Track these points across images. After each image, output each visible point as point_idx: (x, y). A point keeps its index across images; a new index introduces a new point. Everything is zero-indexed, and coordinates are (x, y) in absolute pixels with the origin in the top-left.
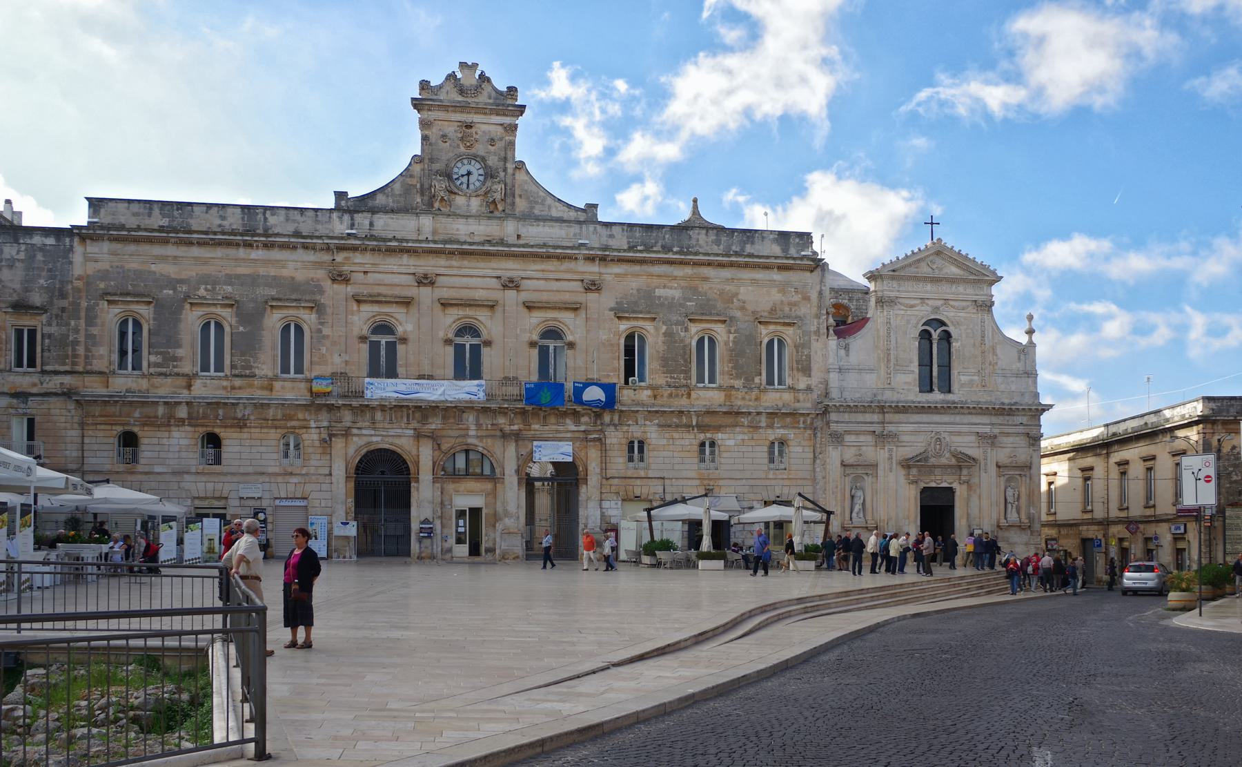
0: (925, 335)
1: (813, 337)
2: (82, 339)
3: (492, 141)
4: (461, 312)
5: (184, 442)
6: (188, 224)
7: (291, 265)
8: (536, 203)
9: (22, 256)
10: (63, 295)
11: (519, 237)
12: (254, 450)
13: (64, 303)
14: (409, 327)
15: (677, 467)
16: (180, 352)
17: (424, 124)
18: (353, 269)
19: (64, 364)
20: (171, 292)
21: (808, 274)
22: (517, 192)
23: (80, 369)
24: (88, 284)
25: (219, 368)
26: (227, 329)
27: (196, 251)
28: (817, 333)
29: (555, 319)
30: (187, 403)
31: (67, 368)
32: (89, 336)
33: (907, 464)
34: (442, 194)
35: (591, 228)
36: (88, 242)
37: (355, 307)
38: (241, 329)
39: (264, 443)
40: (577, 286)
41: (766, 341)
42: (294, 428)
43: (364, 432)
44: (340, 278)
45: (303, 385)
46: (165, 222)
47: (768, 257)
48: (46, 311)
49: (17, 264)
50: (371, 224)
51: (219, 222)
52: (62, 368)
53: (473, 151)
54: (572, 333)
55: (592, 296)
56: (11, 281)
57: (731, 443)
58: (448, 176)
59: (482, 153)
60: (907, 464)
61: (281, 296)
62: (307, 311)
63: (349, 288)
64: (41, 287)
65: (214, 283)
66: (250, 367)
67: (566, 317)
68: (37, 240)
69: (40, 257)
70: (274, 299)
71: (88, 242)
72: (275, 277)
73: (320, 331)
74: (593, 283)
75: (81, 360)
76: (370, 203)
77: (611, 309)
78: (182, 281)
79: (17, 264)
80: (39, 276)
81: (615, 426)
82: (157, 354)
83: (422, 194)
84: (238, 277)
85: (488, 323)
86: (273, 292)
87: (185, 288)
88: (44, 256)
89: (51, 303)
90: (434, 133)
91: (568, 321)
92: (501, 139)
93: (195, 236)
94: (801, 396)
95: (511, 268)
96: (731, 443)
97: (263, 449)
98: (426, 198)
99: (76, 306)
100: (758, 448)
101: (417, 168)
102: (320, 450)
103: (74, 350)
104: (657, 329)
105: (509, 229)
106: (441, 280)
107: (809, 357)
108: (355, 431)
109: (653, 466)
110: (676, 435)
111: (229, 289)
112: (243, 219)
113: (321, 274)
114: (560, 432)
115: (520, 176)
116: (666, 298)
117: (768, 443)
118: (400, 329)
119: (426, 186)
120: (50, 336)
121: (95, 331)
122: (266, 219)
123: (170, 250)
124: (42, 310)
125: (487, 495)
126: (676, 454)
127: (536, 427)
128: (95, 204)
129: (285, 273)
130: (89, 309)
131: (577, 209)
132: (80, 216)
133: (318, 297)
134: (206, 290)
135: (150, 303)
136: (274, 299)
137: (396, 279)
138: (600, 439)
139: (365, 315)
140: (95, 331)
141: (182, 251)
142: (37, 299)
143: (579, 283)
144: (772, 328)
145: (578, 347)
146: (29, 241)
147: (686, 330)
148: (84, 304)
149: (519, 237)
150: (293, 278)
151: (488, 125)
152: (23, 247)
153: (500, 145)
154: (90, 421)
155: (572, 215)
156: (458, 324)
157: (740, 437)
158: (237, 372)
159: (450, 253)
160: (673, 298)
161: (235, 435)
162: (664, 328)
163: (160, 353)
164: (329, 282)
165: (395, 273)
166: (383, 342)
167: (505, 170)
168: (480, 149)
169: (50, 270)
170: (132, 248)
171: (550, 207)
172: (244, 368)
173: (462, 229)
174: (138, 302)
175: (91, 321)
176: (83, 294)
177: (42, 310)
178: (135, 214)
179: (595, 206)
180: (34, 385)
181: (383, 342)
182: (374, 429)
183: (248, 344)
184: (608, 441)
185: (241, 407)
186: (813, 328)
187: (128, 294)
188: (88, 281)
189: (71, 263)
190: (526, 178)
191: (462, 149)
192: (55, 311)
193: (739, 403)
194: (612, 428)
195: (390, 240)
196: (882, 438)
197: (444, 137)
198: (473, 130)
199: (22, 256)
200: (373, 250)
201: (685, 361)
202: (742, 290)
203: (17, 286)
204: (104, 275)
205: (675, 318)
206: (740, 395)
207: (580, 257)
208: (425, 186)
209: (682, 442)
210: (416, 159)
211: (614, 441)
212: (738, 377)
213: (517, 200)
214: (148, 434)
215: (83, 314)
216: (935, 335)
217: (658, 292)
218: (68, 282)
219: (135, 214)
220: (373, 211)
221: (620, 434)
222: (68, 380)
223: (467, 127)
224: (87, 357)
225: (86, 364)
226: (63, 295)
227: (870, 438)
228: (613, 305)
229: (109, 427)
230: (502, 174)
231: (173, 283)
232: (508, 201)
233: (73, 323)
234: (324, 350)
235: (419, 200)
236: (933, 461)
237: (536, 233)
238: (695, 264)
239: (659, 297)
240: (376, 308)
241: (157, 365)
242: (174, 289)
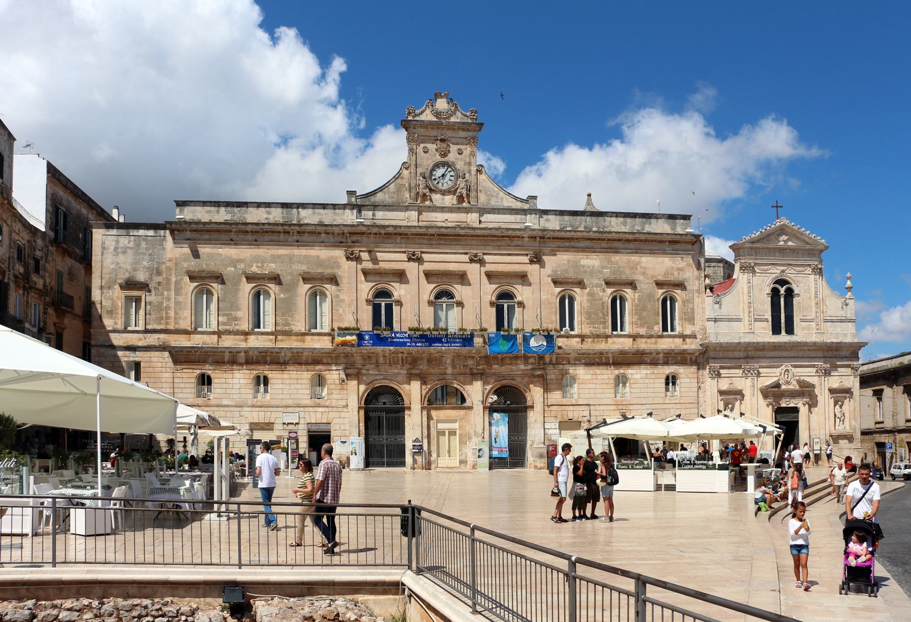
2: (172, 305)
5: (242, 381)
6: (244, 218)
8: (492, 196)
9: (132, 245)
10: (159, 273)
13: (159, 279)
14: (402, 292)
15: (599, 396)
16: (239, 314)
19: (160, 324)
23: (171, 327)
24: (176, 264)
31: (162, 327)
32: (177, 303)
34: (425, 191)
38: (282, 295)
47: (662, 234)
51: (265, 216)
54: (521, 295)
56: (125, 263)
57: (638, 376)
64: (145, 267)
65: (263, 262)
66: (288, 325)
69: (143, 245)
73: (337, 296)
75: (172, 321)
76: (372, 199)
77: (549, 276)
78: (240, 261)
82: (224, 315)
87: (242, 266)
88: (146, 244)
89: (151, 279)
96: (638, 376)
98: (412, 194)
99: (168, 280)
101: (405, 173)
103: (167, 313)
105: (472, 219)
109: (582, 396)
111: (273, 266)
116: (589, 267)
117: (665, 376)
120: (150, 303)
122: (298, 213)
126: (598, 386)
127: (496, 366)
130: (177, 283)
131: (522, 200)
133: (336, 271)
134: (257, 267)
138: (542, 376)
142: (141, 277)
147: (604, 291)
148: (173, 279)
150: (318, 257)
155: (519, 205)
157: (645, 372)
159: (431, 235)
160: (594, 267)
161: (279, 376)
163: (226, 315)
164: (345, 259)
166: (383, 304)
167: (470, 172)
169: (150, 255)
171: (502, 199)
172: (283, 325)
173: (439, 219)
175: (178, 292)
180: (140, 340)
181: (383, 304)
184: (548, 377)
189: (164, 249)
199: (132, 245)
200: (376, 234)
201: (604, 314)
203: (129, 267)
209: (602, 377)
211: (553, 377)
212: (642, 326)
214: (218, 375)
215: (173, 286)
220: (375, 207)
221: (557, 372)
224: (175, 318)
225: (176, 323)
226: (159, 273)
230: (467, 175)
233: (166, 293)
234: (341, 311)
235: (408, 196)
237: (492, 221)
239: (584, 266)
241: (224, 324)
242: (235, 267)
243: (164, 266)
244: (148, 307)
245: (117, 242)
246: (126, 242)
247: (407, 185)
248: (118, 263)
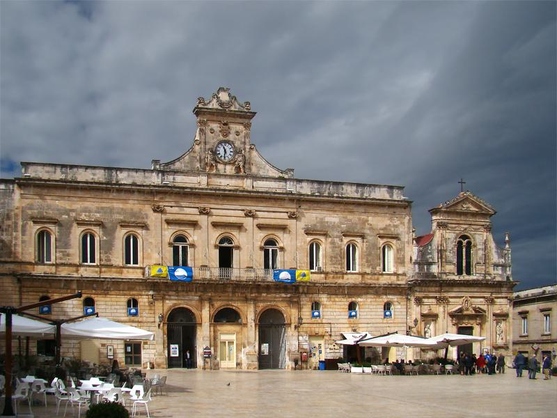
0: (460, 243)
1: (406, 245)
3: (238, 133)
10: (8, 217)
12: (113, 307)
13: (9, 222)
16: (71, 251)
24: (22, 211)
25: (93, 260)
26: (97, 239)
28: (408, 243)
30: (77, 280)
32: (23, 242)
33: (452, 315)
37: (166, 226)
38: (105, 238)
39: (118, 303)
42: (134, 295)
43: (172, 297)
45: (139, 271)
46: (63, 177)
50: (174, 179)
51: (92, 177)
52: (9, 260)
60: (452, 315)
61: (127, 220)
72: (122, 209)
76: (172, 167)
78: (73, 211)
81: (305, 294)
83: (200, 163)
84: (102, 208)
85: (237, 236)
93: (80, 184)
94: (400, 277)
97: (118, 307)
98: (202, 164)
99: (16, 224)
100: (378, 307)
102: (148, 308)
107: (404, 256)
108: (167, 297)
109: (326, 317)
110: (337, 299)
111: (98, 215)
112: (105, 175)
114: (277, 298)
116: (331, 223)
118: (190, 239)
119: (202, 158)
121: (26, 238)
122: (117, 175)
125: (238, 333)
127: (264, 295)
134: (85, 216)
140: (26, 238)
144: (385, 240)
147: (342, 240)
148: (20, 223)
150: (132, 210)
153: (242, 135)
154: (25, 290)
156: (222, 236)
158: (102, 263)
159: (217, 196)
160: (334, 223)
161: (103, 299)
164: (152, 212)
166: (180, 247)
167: (245, 149)
168: (231, 137)
171: (268, 170)
173: (224, 183)
175: (24, 233)
176: (20, 217)
178: (48, 172)
181: (180, 247)
182: (177, 296)
183: (108, 247)
185: (106, 283)
186: (406, 240)
189: (13, 199)
191: (221, 137)
193: (369, 280)
194: (304, 296)
196: (441, 300)
197: (212, 131)
201: (341, 258)
205: (336, 234)
206: (369, 277)
209: (340, 303)
212: (368, 267)
215: (20, 229)
217: (327, 219)
218: (12, 210)
219: (48, 172)
220: (176, 172)
222: (12, 266)
227: (434, 300)
229: (35, 294)
231: (67, 212)
233: (14, 234)
234: (149, 250)
236: (465, 313)
238: (346, 203)
240: (178, 228)
241: (61, 259)
242: (69, 215)
247: (198, 158)
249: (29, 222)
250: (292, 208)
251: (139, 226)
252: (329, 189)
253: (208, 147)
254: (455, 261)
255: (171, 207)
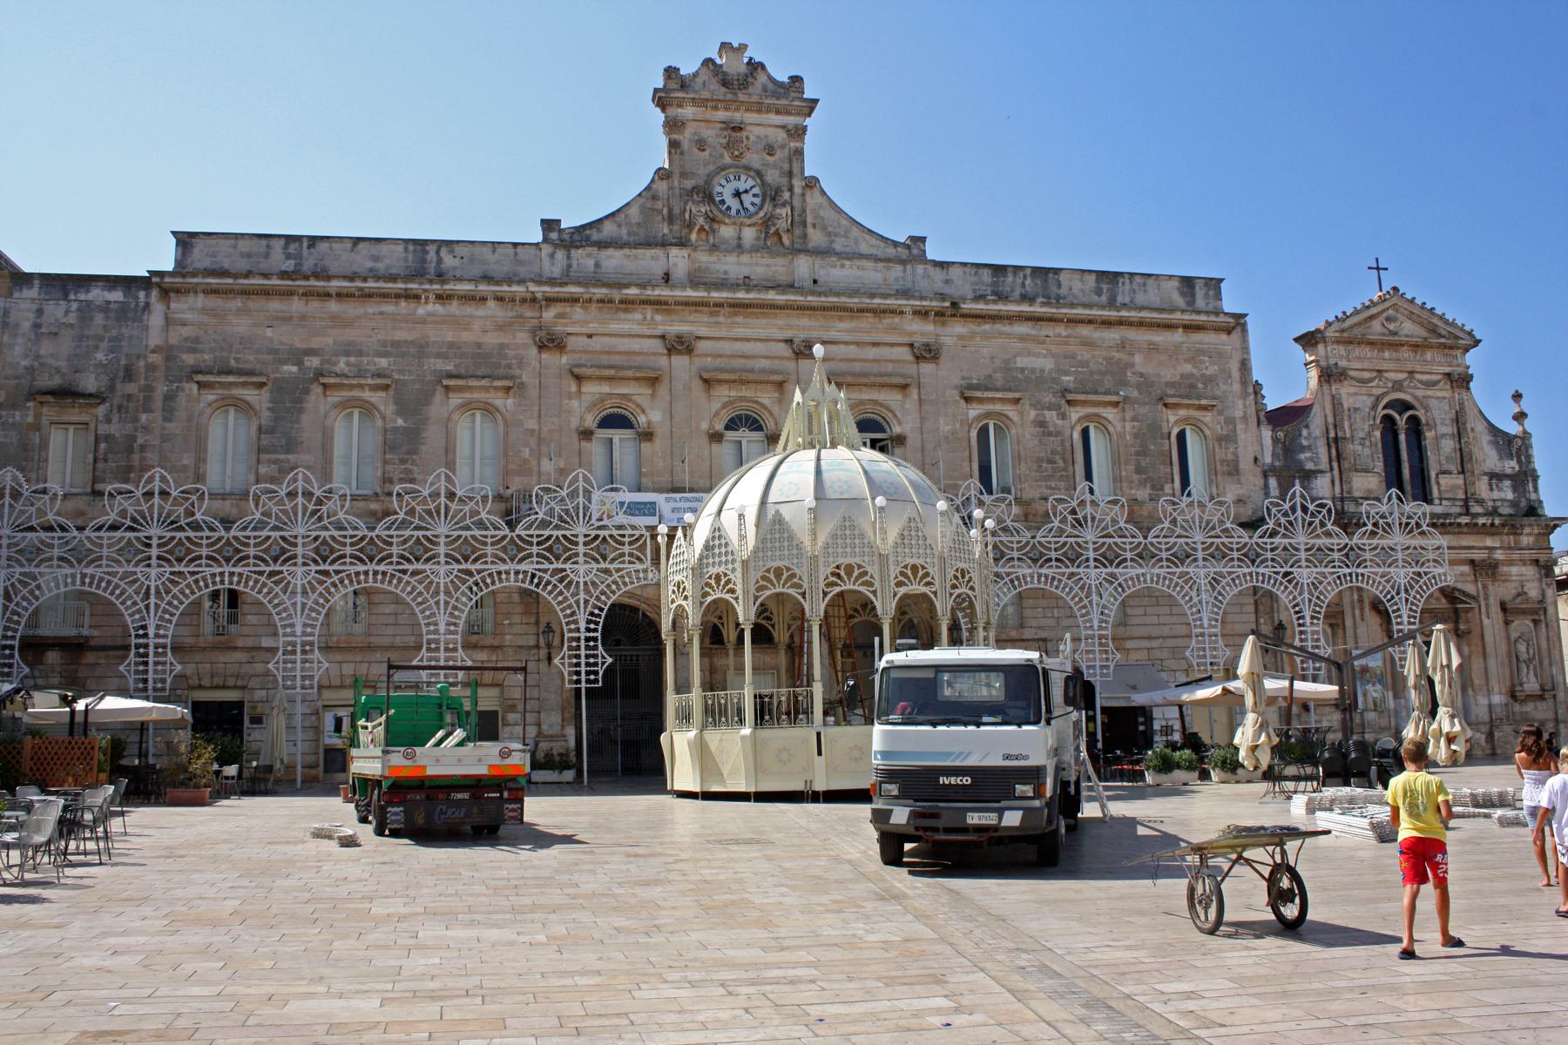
0: (1388, 422)
1: (1240, 427)
3: (770, 150)
4: (733, 393)
7: (477, 325)
10: (129, 375)
11: (815, 282)
13: (131, 388)
17: (672, 125)
18: (569, 330)
20: (295, 369)
21: (1224, 337)
22: (809, 220)
24: (168, 358)
27: (333, 306)
29: (875, 402)
35: (920, 269)
36: (172, 295)
38: (400, 422)
40: (904, 354)
41: (1175, 431)
44: (551, 342)
48: (103, 400)
49: (63, 332)
51: (369, 264)
53: (744, 161)
55: (927, 368)
58: (708, 197)
59: (756, 165)
62: (500, 394)
63: (564, 359)
64: (101, 365)
67: (891, 398)
68: (96, 294)
69: (99, 319)
70: (451, 376)
71: (172, 295)
72: (451, 345)
74: (928, 347)
79: (63, 332)
80: (97, 348)
86: (450, 367)
89: (112, 388)
90: (686, 137)
91: (894, 405)
92: (783, 147)
95: (801, 326)
99: (149, 389)
101: (662, 187)
104: (1021, 413)
105: (803, 267)
106: (701, 346)
111: (383, 362)
113: (523, 337)
115: (813, 199)
116: (1033, 371)
118: (642, 419)
119: (677, 211)
120: (108, 438)
122: (440, 260)
123: (296, 305)
124: (98, 398)
128: (185, 241)
129: (466, 337)
130: (169, 398)
131: (895, 244)
132: (165, 259)
135: (262, 385)
136: (451, 376)
137: (636, 345)
139: (587, 399)
141: (314, 305)
142: (89, 383)
143: (906, 350)
144: (1182, 412)
145: (909, 442)
146: (82, 297)
147: (1063, 416)
148: (161, 388)
149: (815, 282)
150: (479, 345)
151: (764, 126)
152: (75, 306)
155: (891, 251)
159: (716, 305)
160: (1042, 371)
162: (1033, 414)
163: (276, 462)
164: (534, 350)
165: (632, 334)
167: (791, 189)
168: (754, 159)
170: (237, 303)
171: (856, 242)
173: (732, 266)
174: (244, 384)
176: (160, 374)
177: (98, 398)
179: (923, 240)
186: (1239, 413)
187: (229, 372)
188: (168, 352)
189: (147, 328)
190: (820, 199)
192: (116, 401)
195: (627, 286)
197: (701, 144)
198: (744, 134)
200: (601, 301)
202: (1138, 359)
204: (193, 345)
205: (1048, 398)
207: (908, 309)
208: (677, 207)
210: (661, 174)
212: (1142, 484)
213: (810, 230)
215: (158, 403)
216: (1401, 421)
217: (1021, 362)
220: (602, 245)
223: (733, 129)
226: (129, 375)
228: (956, 381)
231: (297, 356)
232: (797, 232)
233: (144, 417)
237: (839, 274)
238: (1070, 321)
239: (1023, 370)
242: (300, 363)
243: (142, 363)
244: (103, 446)
245: (40, 312)
246: (60, 313)
247: (665, 211)
248: (38, 357)
249: (187, 386)
250: (923, 330)
251: (496, 388)
252: (1023, 285)
253: (689, 184)
254: (1379, 466)
255: (590, 336)
